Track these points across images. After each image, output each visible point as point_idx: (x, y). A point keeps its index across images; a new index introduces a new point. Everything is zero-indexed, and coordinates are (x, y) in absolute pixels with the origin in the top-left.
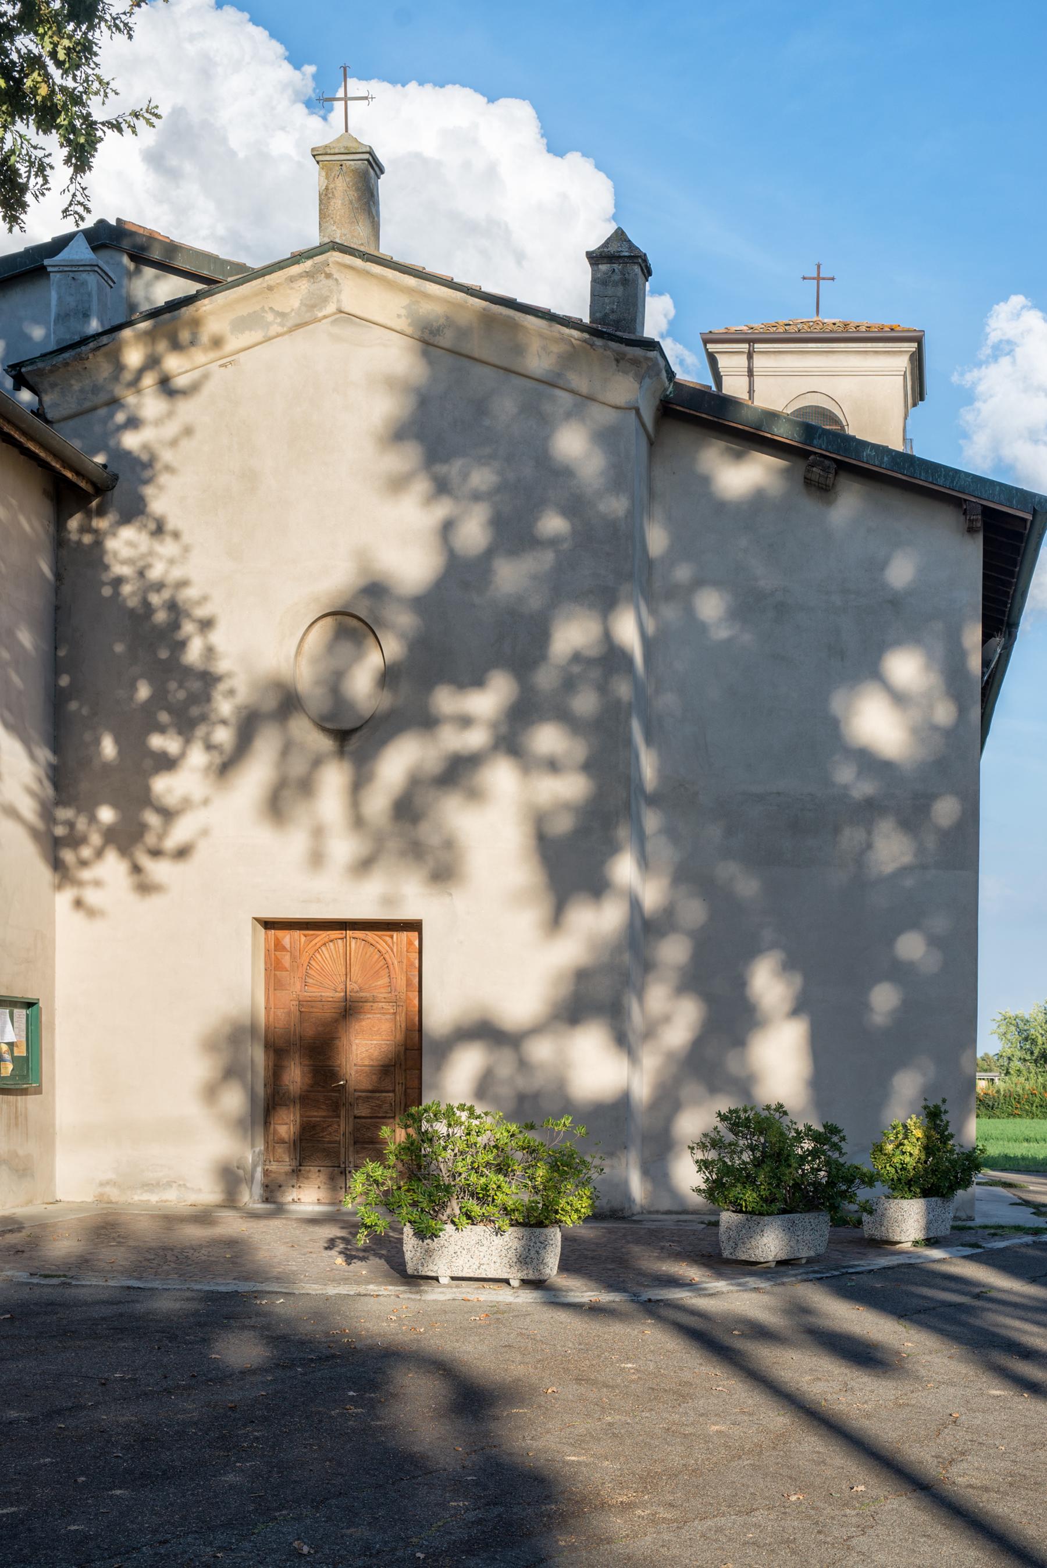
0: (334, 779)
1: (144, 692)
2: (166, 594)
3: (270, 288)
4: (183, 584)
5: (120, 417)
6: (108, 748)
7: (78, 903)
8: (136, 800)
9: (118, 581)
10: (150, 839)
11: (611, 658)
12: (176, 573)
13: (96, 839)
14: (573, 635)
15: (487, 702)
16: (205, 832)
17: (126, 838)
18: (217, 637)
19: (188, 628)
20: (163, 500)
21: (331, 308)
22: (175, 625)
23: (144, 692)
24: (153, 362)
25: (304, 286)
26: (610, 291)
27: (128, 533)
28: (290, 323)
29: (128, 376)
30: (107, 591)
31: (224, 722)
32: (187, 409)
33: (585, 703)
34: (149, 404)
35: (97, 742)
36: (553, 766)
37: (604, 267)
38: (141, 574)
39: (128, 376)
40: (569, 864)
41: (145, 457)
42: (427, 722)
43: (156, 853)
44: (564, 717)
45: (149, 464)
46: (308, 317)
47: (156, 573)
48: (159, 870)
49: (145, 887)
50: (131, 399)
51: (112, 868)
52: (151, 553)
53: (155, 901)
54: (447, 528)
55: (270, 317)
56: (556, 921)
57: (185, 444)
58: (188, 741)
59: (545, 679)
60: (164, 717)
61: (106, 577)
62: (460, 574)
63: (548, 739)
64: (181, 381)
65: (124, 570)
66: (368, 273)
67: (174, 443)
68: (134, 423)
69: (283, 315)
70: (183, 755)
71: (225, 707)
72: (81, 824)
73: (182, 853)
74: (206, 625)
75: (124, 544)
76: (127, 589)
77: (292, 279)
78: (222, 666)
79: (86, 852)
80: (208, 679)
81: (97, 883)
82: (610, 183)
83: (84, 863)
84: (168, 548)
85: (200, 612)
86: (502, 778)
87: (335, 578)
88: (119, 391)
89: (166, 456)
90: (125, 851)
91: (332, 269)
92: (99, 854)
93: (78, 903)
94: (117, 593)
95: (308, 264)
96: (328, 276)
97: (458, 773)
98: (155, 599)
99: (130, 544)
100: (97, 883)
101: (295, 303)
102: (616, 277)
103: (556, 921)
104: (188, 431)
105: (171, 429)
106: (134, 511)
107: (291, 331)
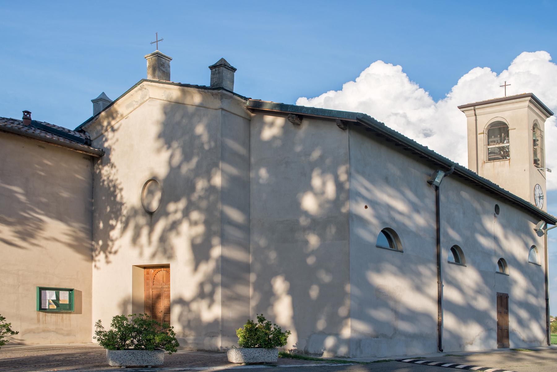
0: (145, 232)
1: (108, 209)
2: (113, 183)
3: (132, 95)
4: (117, 180)
5: (104, 139)
6: (101, 225)
7: (95, 266)
8: (107, 238)
9: (104, 181)
10: (109, 249)
11: (211, 189)
12: (115, 177)
13: (99, 249)
14: (201, 184)
15: (182, 205)
16: (120, 247)
17: (105, 248)
18: (123, 193)
19: (117, 191)
20: (114, 157)
21: (147, 98)
22: (115, 191)
23: (108, 209)
24: (109, 123)
25: (140, 93)
26: (215, 76)
27: (106, 168)
28: (139, 103)
29: (104, 128)
30: (101, 184)
31: (124, 216)
32: (117, 134)
33: (204, 204)
34: (109, 135)
35: (99, 223)
36: (195, 223)
37: (214, 70)
38: (108, 178)
39: (104, 128)
40: (200, 252)
41: (109, 148)
42: (167, 214)
43: (110, 253)
44: (198, 208)
45: (111, 149)
46: (142, 101)
47: (111, 178)
48: (111, 257)
49: (108, 262)
50: (106, 134)
51: (102, 256)
52: (110, 173)
53: (110, 265)
54: (172, 157)
55: (134, 103)
56: (196, 269)
57: (117, 143)
58: (117, 221)
59: (195, 197)
60: (113, 216)
61: (101, 180)
62: (174, 170)
63: (195, 215)
64: (116, 127)
65: (105, 178)
66: (152, 86)
67: (114, 143)
68: (106, 140)
69: (137, 102)
70: (116, 225)
71: (124, 212)
72: (96, 246)
73: (116, 252)
74: (121, 190)
75: (105, 171)
76: (106, 183)
77: (136, 92)
78: (124, 201)
79: (97, 252)
80: (122, 204)
81: (99, 261)
82: (379, 62)
83: (96, 256)
84: (114, 171)
85: (120, 187)
86: (185, 227)
87: (145, 176)
88: (103, 131)
89: (113, 147)
90: (105, 252)
91: (145, 87)
92: (99, 253)
93: (95, 266)
94: (103, 184)
95: (139, 87)
96: (145, 89)
97: (174, 226)
98: (111, 184)
99: (107, 171)
100: (99, 261)
101: (139, 98)
102: (217, 72)
103: (196, 269)
104: (117, 140)
105: (114, 140)
106: (107, 162)
107: (140, 106)
